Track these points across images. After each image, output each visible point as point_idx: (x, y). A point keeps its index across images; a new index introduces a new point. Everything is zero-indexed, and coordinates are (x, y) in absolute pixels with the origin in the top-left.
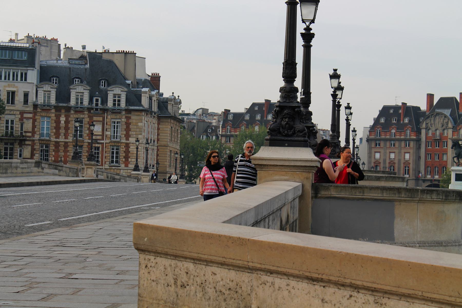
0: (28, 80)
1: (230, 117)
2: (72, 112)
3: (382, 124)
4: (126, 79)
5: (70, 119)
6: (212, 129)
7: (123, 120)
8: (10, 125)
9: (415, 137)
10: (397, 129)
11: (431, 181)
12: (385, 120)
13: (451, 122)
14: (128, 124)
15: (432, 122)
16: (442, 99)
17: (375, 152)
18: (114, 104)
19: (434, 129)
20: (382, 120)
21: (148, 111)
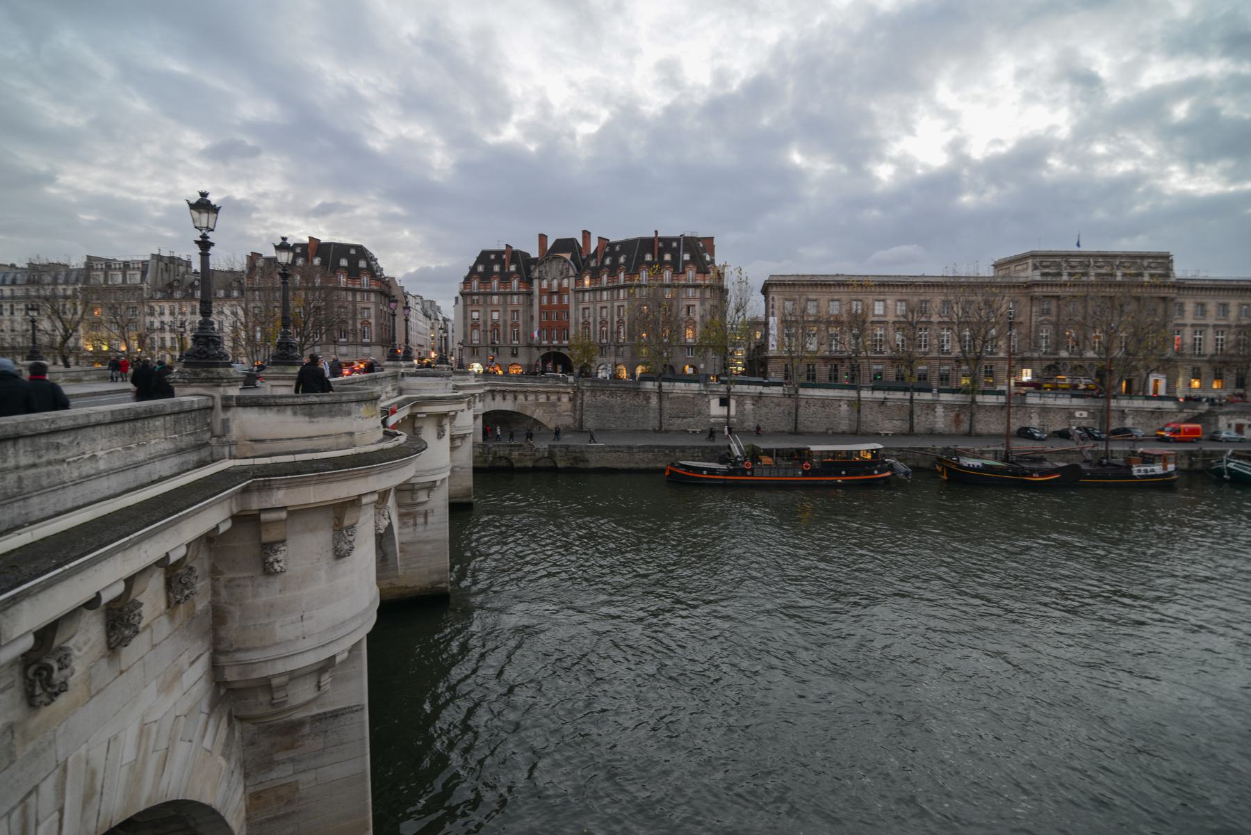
1: (260, 263)
10: (502, 279)
11: (548, 347)
12: (485, 268)
15: (548, 269)
16: (558, 241)
20: (480, 268)
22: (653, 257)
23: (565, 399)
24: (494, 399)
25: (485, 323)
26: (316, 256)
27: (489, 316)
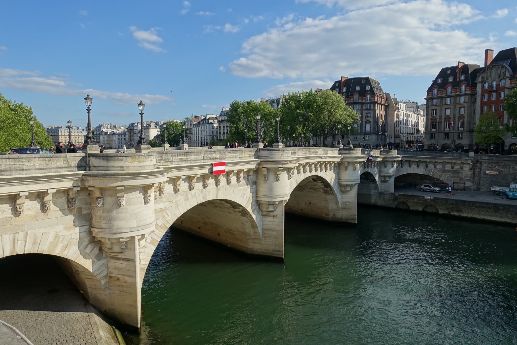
3: (439, 84)
9: (470, 92)
12: (443, 81)
13: (509, 71)
15: (489, 74)
19: (490, 82)
20: (440, 81)
23: (466, 168)
24: (410, 166)
27: (443, 112)
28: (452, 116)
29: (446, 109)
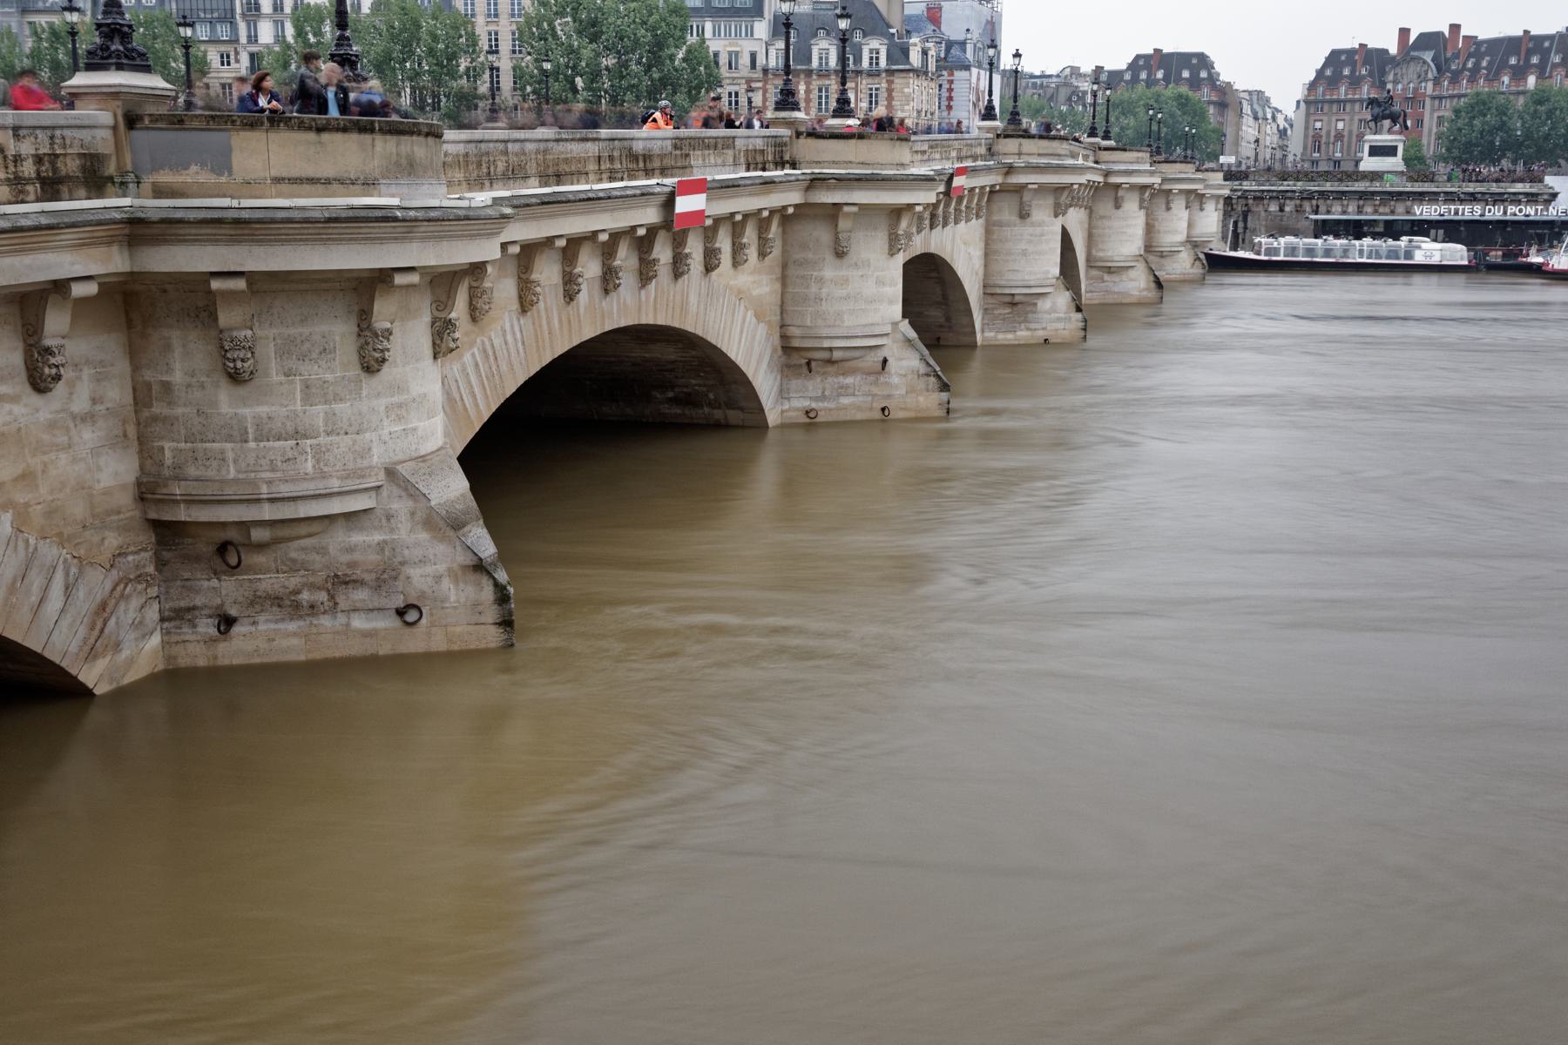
0: (756, 36)
1: (1104, 77)
2: (814, 77)
4: (890, 27)
5: (812, 87)
6: (1078, 96)
7: (883, 85)
8: (733, 99)
10: (1350, 84)
12: (1333, 72)
13: (1432, 71)
14: (890, 91)
15: (1404, 71)
16: (1422, 36)
17: (1315, 121)
18: (871, 64)
19: (1406, 83)
20: (1328, 72)
21: (921, 72)
22: (1519, 61)
25: (1328, 133)
26: (1159, 68)
27: (1333, 125)
28: (1346, 133)
29: (1337, 120)
